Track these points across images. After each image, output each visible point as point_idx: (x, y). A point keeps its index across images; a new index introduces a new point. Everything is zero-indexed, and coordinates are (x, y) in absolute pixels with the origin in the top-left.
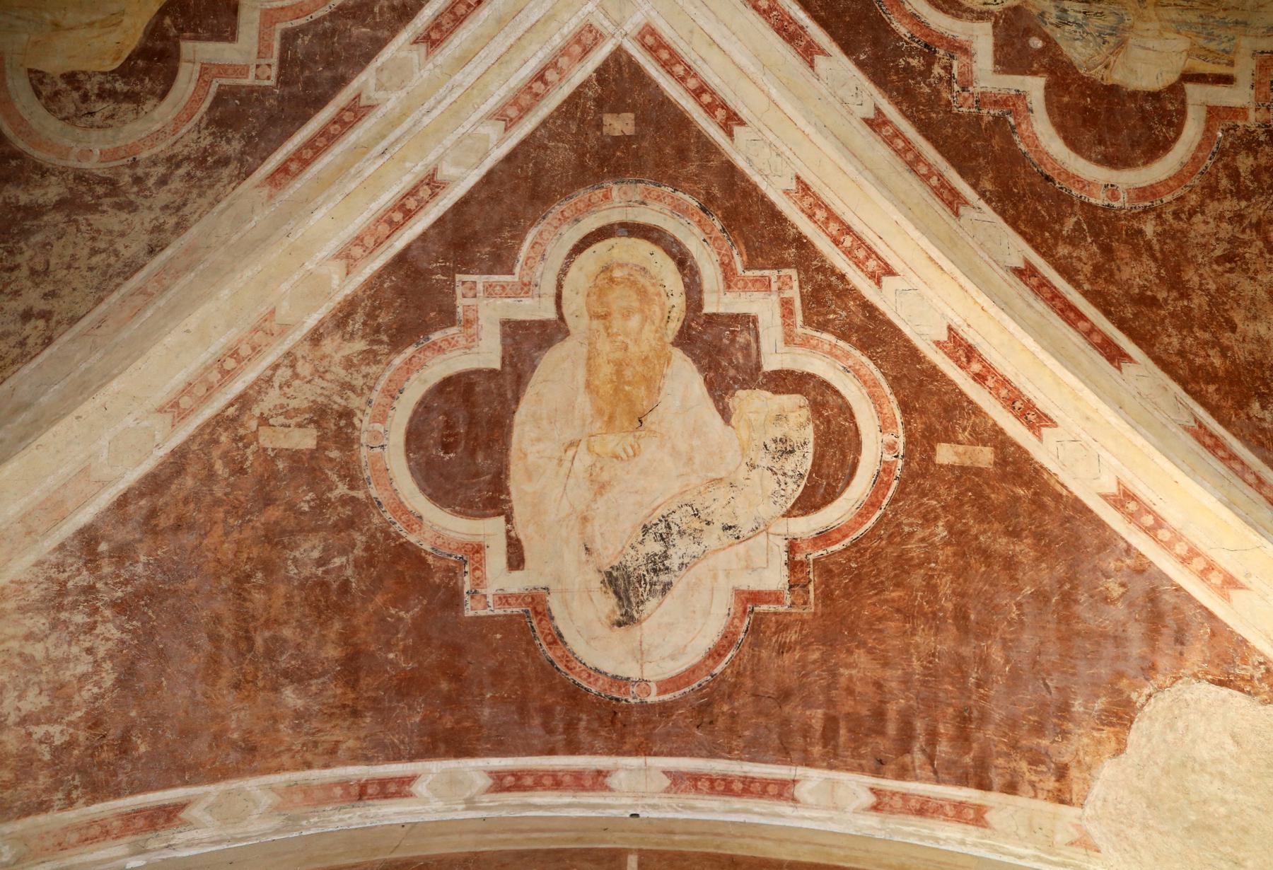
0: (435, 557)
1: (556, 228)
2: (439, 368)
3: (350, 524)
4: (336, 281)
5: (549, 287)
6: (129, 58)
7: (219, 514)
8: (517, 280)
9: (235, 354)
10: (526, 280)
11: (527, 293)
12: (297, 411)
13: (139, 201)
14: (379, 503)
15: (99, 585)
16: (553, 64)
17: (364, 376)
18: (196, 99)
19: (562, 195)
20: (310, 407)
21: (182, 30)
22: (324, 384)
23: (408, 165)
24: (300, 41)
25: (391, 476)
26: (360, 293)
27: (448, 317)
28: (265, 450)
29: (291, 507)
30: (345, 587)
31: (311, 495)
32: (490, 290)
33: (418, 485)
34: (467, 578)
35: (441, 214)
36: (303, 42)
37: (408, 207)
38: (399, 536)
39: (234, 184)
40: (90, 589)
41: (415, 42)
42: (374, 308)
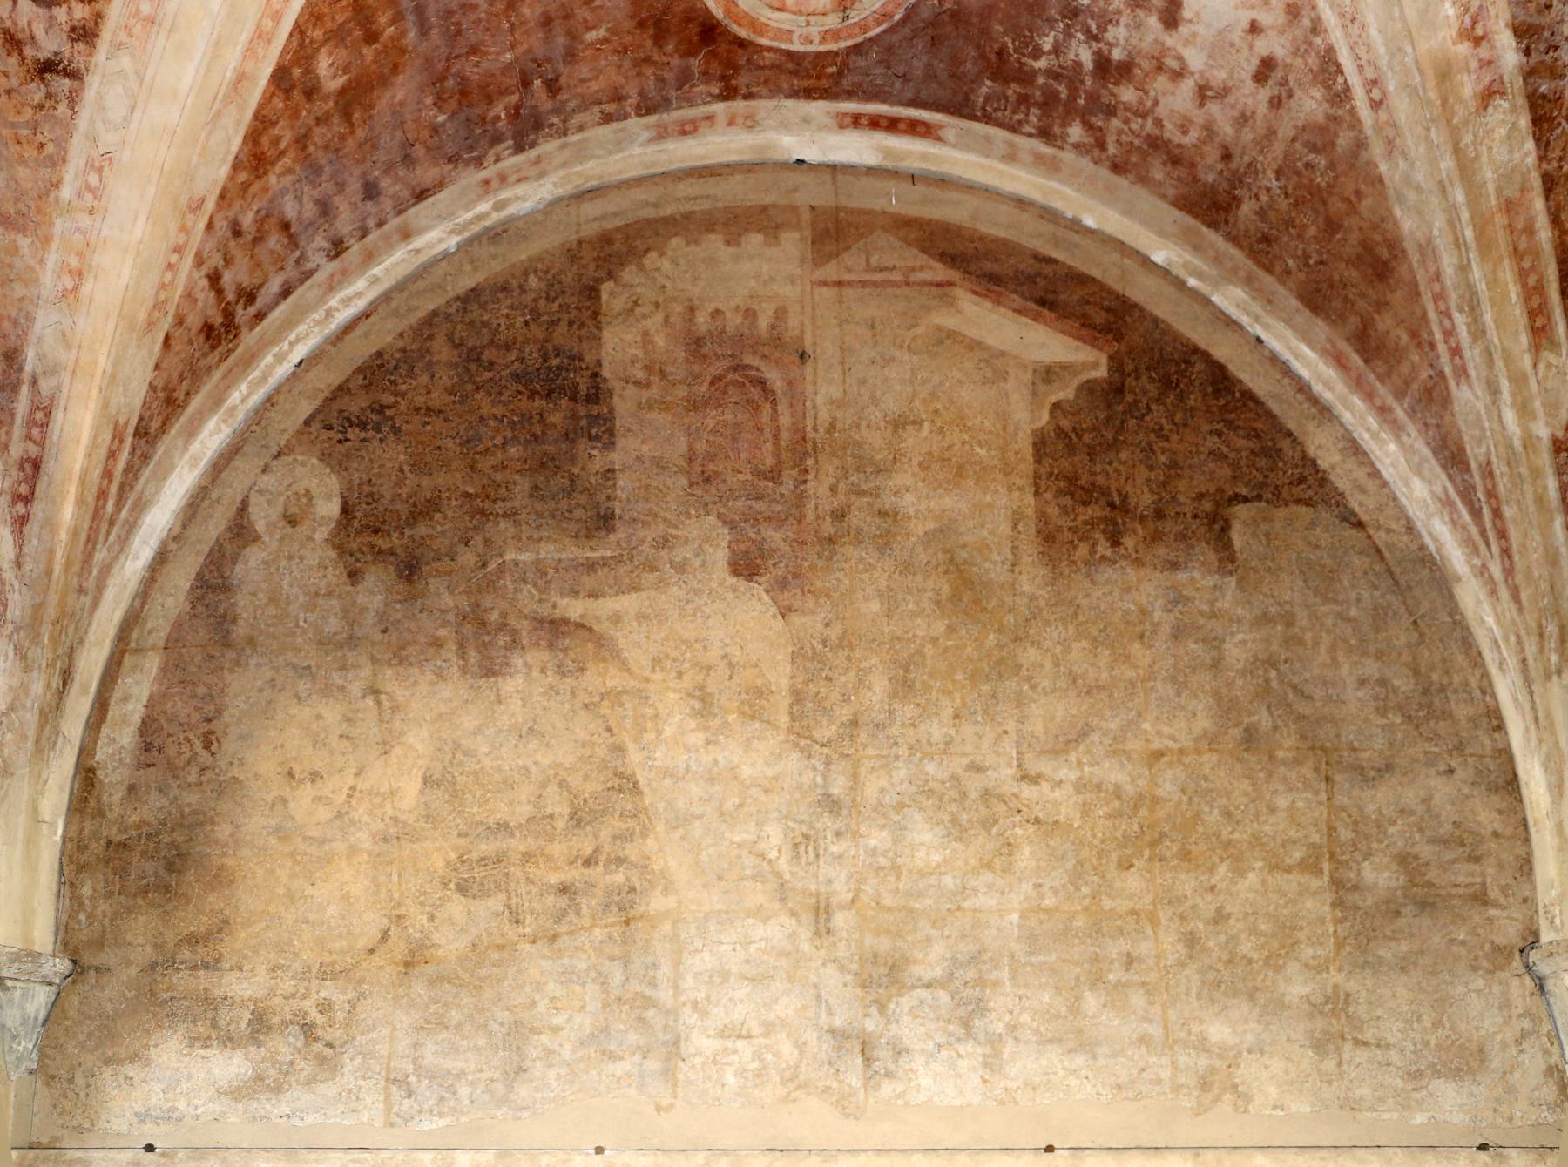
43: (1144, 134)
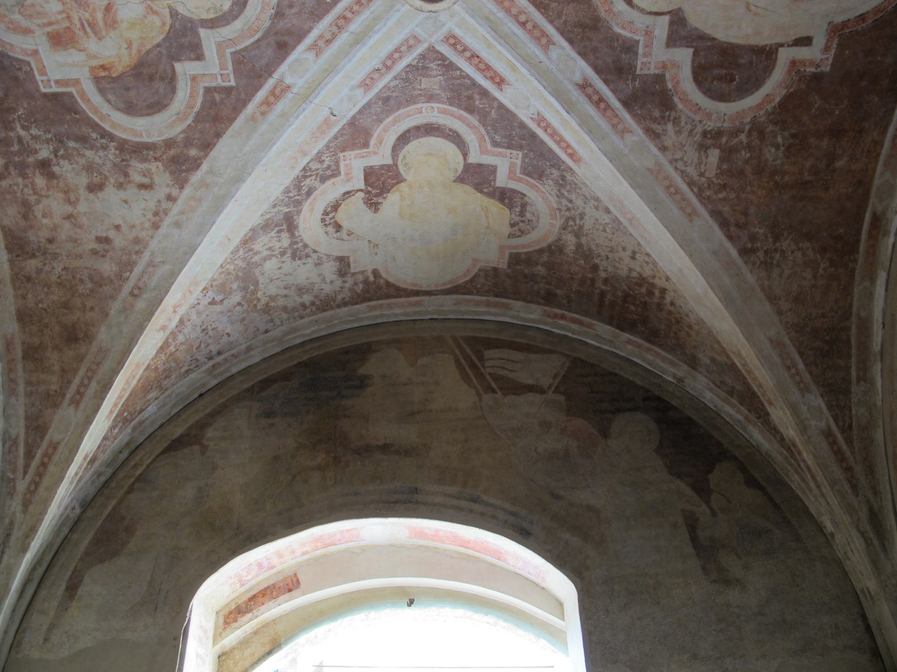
0: (790, 88)
1: (614, 15)
2: (688, 85)
3: (761, 133)
4: (635, 138)
5: (650, 20)
6: (504, 205)
7: (744, 196)
8: (643, 38)
9: (668, 188)
10: (644, 33)
11: (651, 32)
12: (700, 158)
13: (580, 211)
14: (754, 117)
15: (765, 248)
16: (516, 17)
17: (686, 124)
18: (528, 183)
19: (595, 11)
20: (699, 152)
21: (490, 185)
22: (688, 145)
23: (574, 99)
24: (498, 140)
25: (741, 110)
26: (642, 126)
27: (660, 78)
28: (716, 174)
29: (746, 162)
30: (793, 136)
31: (743, 153)
32: (647, 54)
33: (749, 96)
34: (808, 70)
35: (601, 81)
36: (497, 138)
37: (597, 100)
38: (775, 107)
39: (576, 176)
40: (766, 252)
41: (501, 90)
42: (651, 119)
43: (26, 197)
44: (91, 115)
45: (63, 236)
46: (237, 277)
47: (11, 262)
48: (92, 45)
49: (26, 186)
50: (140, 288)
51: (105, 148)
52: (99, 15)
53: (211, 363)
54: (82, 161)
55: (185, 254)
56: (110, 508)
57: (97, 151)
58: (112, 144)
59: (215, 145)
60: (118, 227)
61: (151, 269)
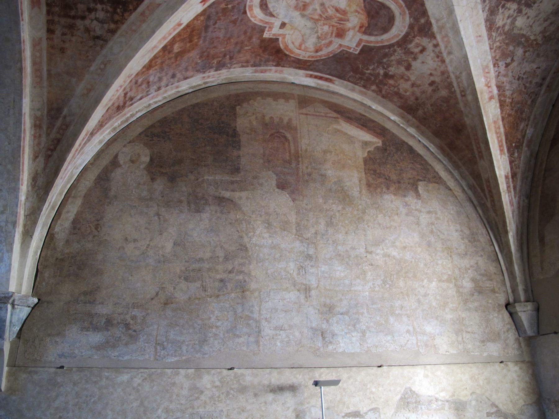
44: (378, 45)
45: (418, 94)
46: (507, 44)
47: (413, 117)
48: (349, 25)
49: (389, 87)
50: (463, 91)
51: (395, 51)
52: (338, 15)
53: (544, 87)
54: (394, 63)
55: (465, 62)
56: (540, 192)
57: (394, 55)
58: (395, 47)
59: (426, 9)
60: (431, 74)
61: (459, 80)
